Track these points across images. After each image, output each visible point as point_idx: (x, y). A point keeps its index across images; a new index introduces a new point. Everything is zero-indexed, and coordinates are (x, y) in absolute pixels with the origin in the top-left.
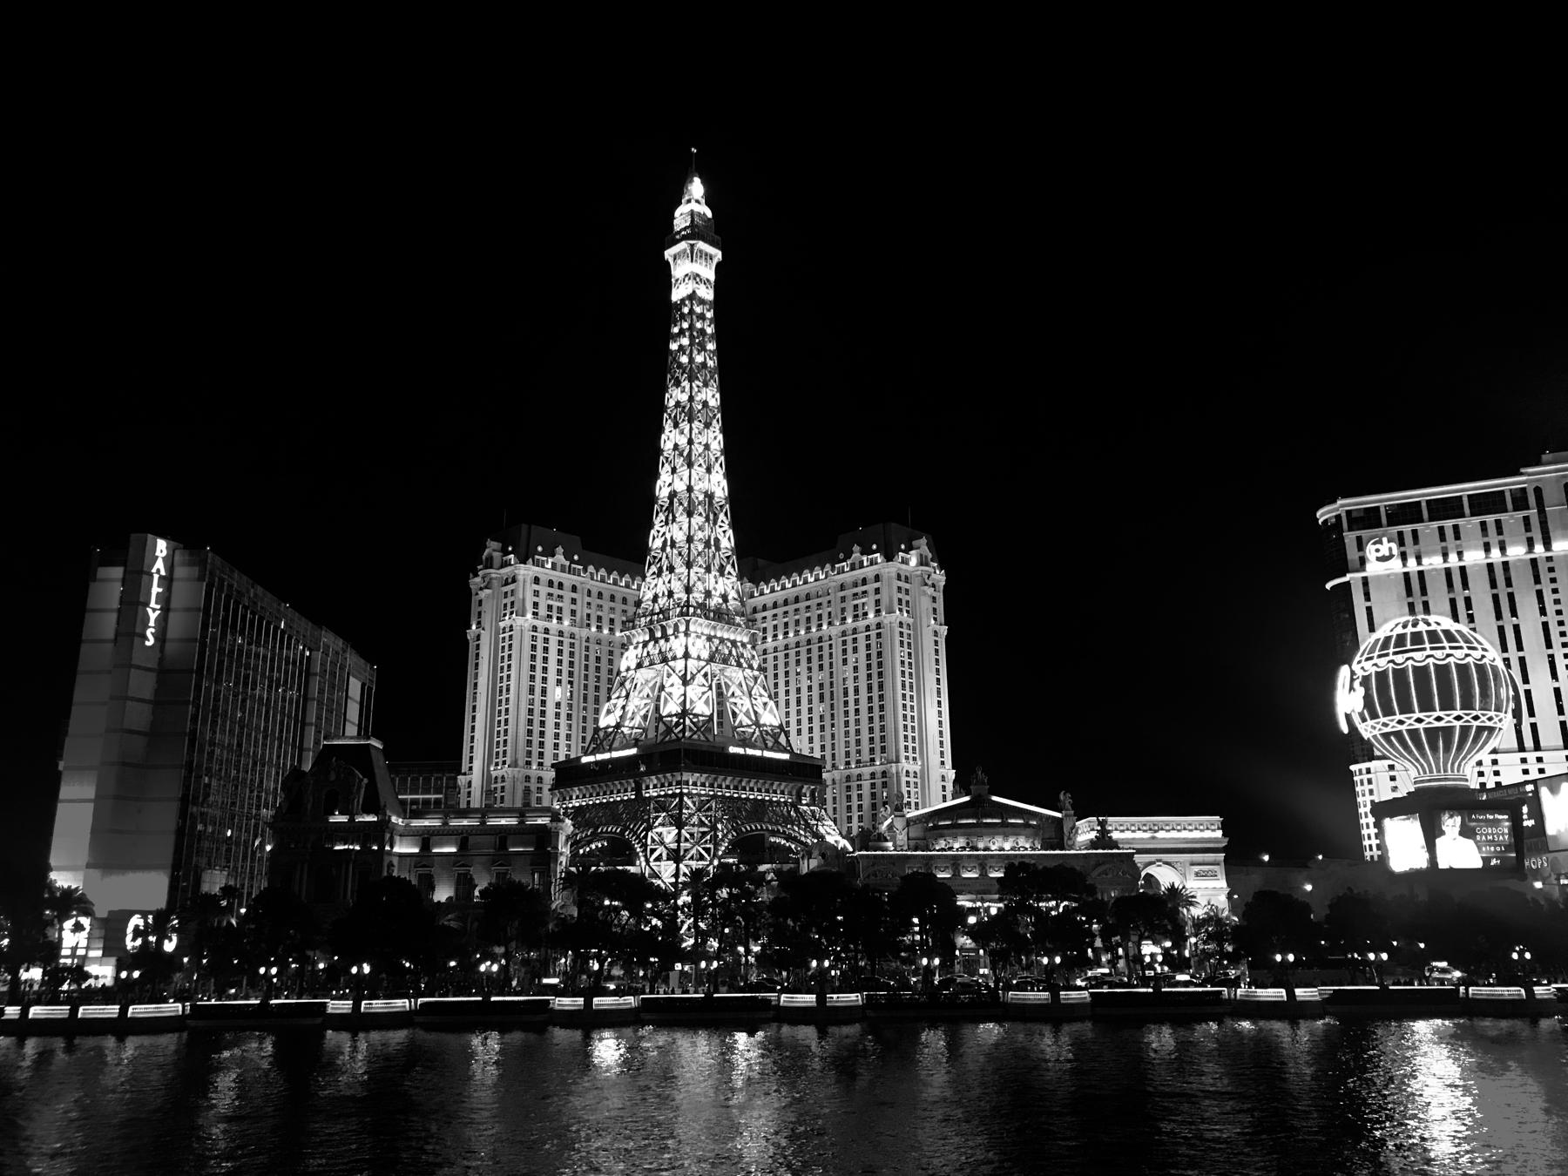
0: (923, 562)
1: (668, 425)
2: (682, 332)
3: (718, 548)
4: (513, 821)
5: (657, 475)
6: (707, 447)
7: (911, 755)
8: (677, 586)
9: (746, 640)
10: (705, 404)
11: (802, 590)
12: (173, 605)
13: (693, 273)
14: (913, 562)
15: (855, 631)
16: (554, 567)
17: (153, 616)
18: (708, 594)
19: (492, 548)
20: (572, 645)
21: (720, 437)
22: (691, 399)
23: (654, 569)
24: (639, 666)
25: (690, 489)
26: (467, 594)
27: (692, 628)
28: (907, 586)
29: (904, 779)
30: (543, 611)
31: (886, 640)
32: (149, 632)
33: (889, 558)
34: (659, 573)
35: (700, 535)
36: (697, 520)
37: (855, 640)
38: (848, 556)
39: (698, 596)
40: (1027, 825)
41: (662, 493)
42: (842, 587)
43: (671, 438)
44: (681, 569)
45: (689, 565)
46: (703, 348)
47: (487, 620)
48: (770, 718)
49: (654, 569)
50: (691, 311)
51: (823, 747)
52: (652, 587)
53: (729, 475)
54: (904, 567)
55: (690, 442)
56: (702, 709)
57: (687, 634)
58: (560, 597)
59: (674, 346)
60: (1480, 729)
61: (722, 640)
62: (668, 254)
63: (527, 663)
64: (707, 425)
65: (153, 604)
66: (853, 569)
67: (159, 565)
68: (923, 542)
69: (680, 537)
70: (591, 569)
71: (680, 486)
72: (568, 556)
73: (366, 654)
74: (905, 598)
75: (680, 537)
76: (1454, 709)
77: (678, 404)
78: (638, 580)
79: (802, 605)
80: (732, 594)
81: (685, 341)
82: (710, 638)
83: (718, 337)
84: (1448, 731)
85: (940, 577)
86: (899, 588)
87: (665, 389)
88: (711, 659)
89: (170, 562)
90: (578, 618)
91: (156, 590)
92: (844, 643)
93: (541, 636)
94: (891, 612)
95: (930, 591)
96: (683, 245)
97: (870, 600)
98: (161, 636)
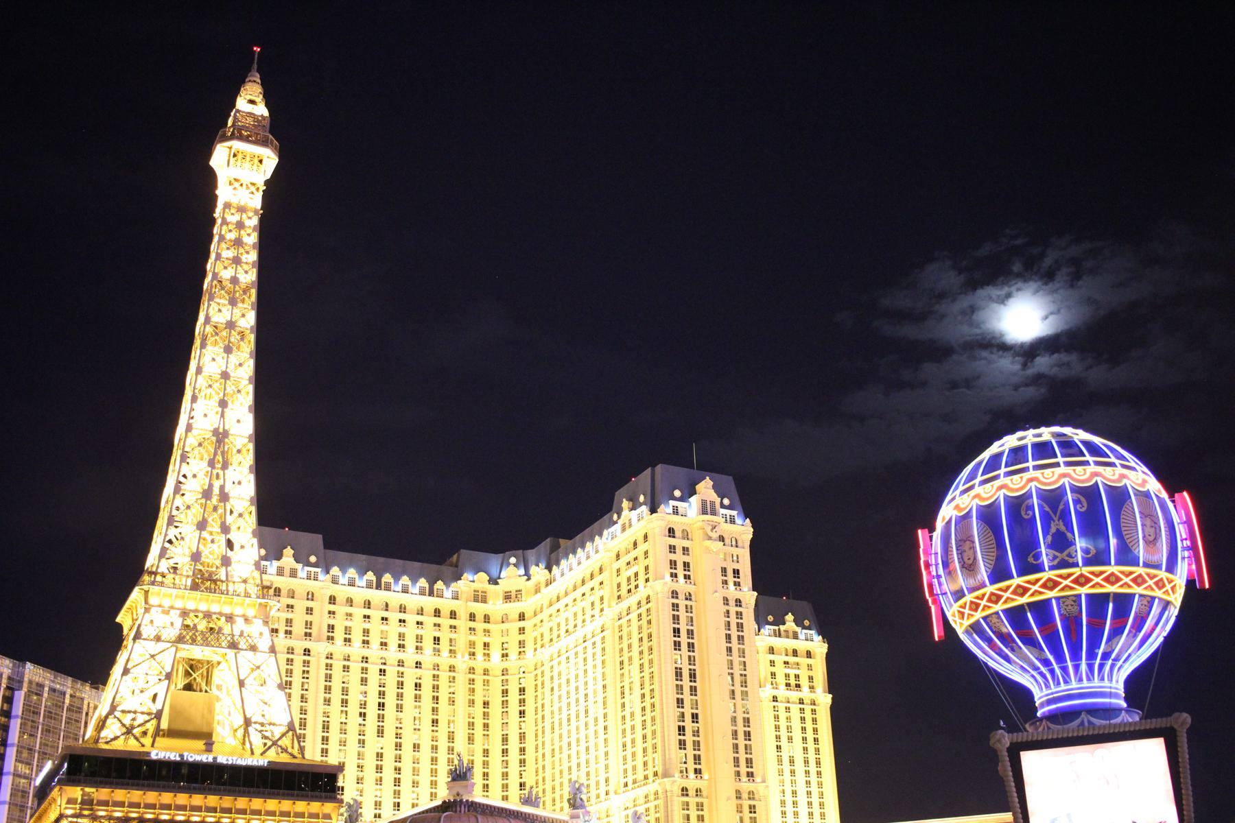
3: (224, 497)
6: (225, 376)
9: (251, 613)
16: (280, 572)
20: (306, 663)
27: (152, 600)
28: (686, 543)
33: (653, 510)
38: (619, 517)
58: (290, 607)
60: (1097, 602)
64: (228, 350)
68: (706, 488)
70: (335, 570)
74: (680, 558)
76: (1039, 568)
83: (264, 246)
84: (1042, 609)
85: (744, 530)
86: (672, 549)
88: (180, 639)
90: (314, 631)
92: (620, 626)
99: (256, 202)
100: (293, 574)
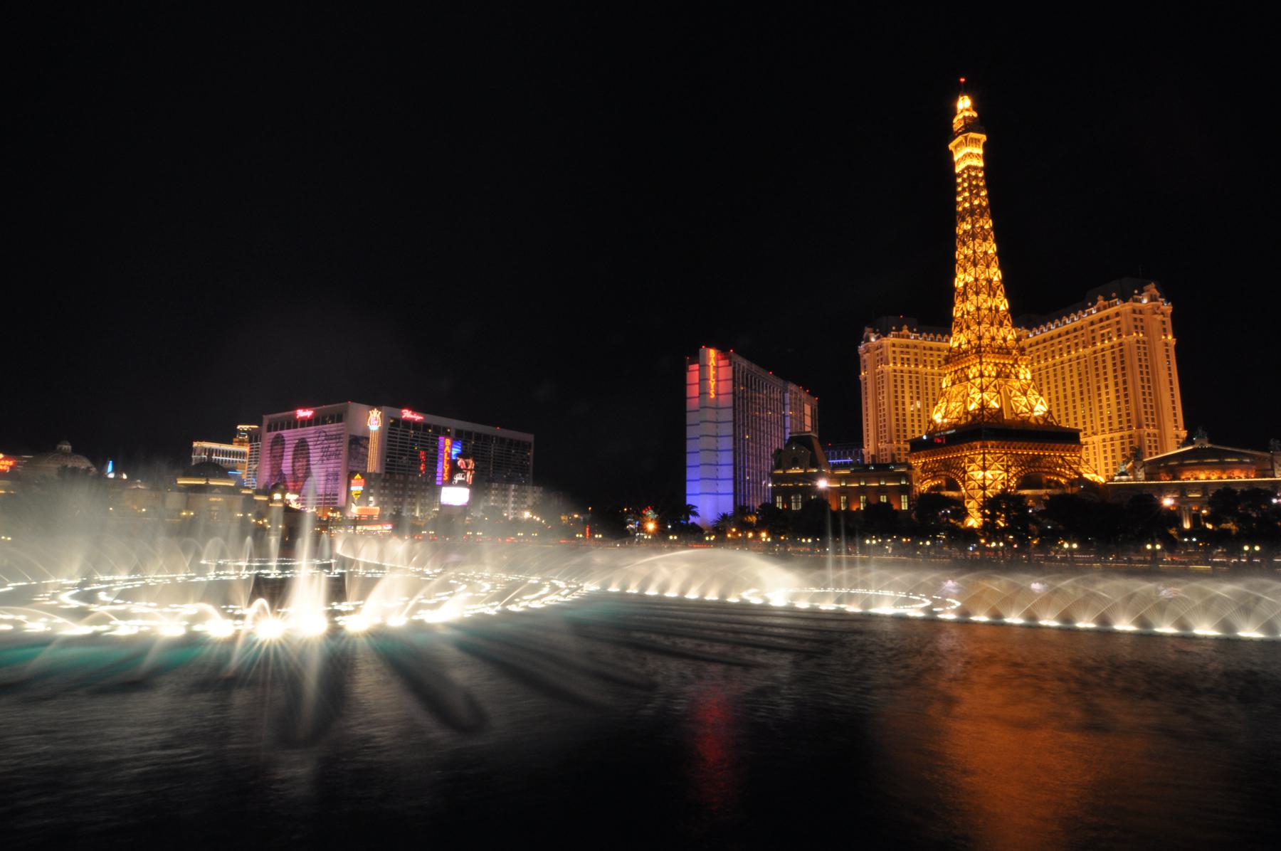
0: (1152, 299)
1: (959, 245)
2: (964, 190)
5: (954, 275)
6: (986, 253)
7: (1150, 423)
8: (973, 337)
10: (982, 228)
11: (1063, 329)
13: (968, 155)
14: (1145, 301)
15: (1103, 350)
17: (712, 384)
18: (993, 339)
19: (868, 330)
21: (994, 246)
22: (973, 227)
23: (958, 329)
24: (954, 383)
25: (976, 280)
26: (857, 357)
29: (1147, 438)
30: (898, 360)
31: (1126, 353)
32: (712, 392)
34: (961, 331)
35: (985, 306)
36: (982, 297)
38: (1094, 303)
39: (985, 341)
40: (1241, 463)
41: (959, 283)
43: (962, 253)
44: (974, 327)
45: (979, 324)
46: (978, 195)
47: (869, 367)
48: (1040, 409)
49: (958, 329)
50: (969, 176)
52: (958, 340)
53: (1001, 267)
55: (975, 252)
56: (994, 404)
57: (981, 363)
59: (959, 199)
61: (1004, 364)
62: (951, 146)
63: (892, 389)
64: (985, 240)
66: (1098, 310)
68: (1152, 288)
69: (972, 309)
71: (970, 279)
72: (911, 330)
73: (812, 394)
74: (1139, 324)
75: (972, 309)
77: (965, 231)
78: (946, 337)
79: (1063, 338)
80: (1009, 337)
81: (967, 194)
82: (996, 364)
83: (987, 186)
85: (1167, 308)
87: (954, 225)
88: (997, 376)
89: (717, 360)
91: (712, 372)
93: (899, 374)
94: (1129, 334)
95: (1160, 317)
96: (960, 138)
97: (1113, 329)
98: (717, 394)
99: (981, 164)
100: (908, 337)
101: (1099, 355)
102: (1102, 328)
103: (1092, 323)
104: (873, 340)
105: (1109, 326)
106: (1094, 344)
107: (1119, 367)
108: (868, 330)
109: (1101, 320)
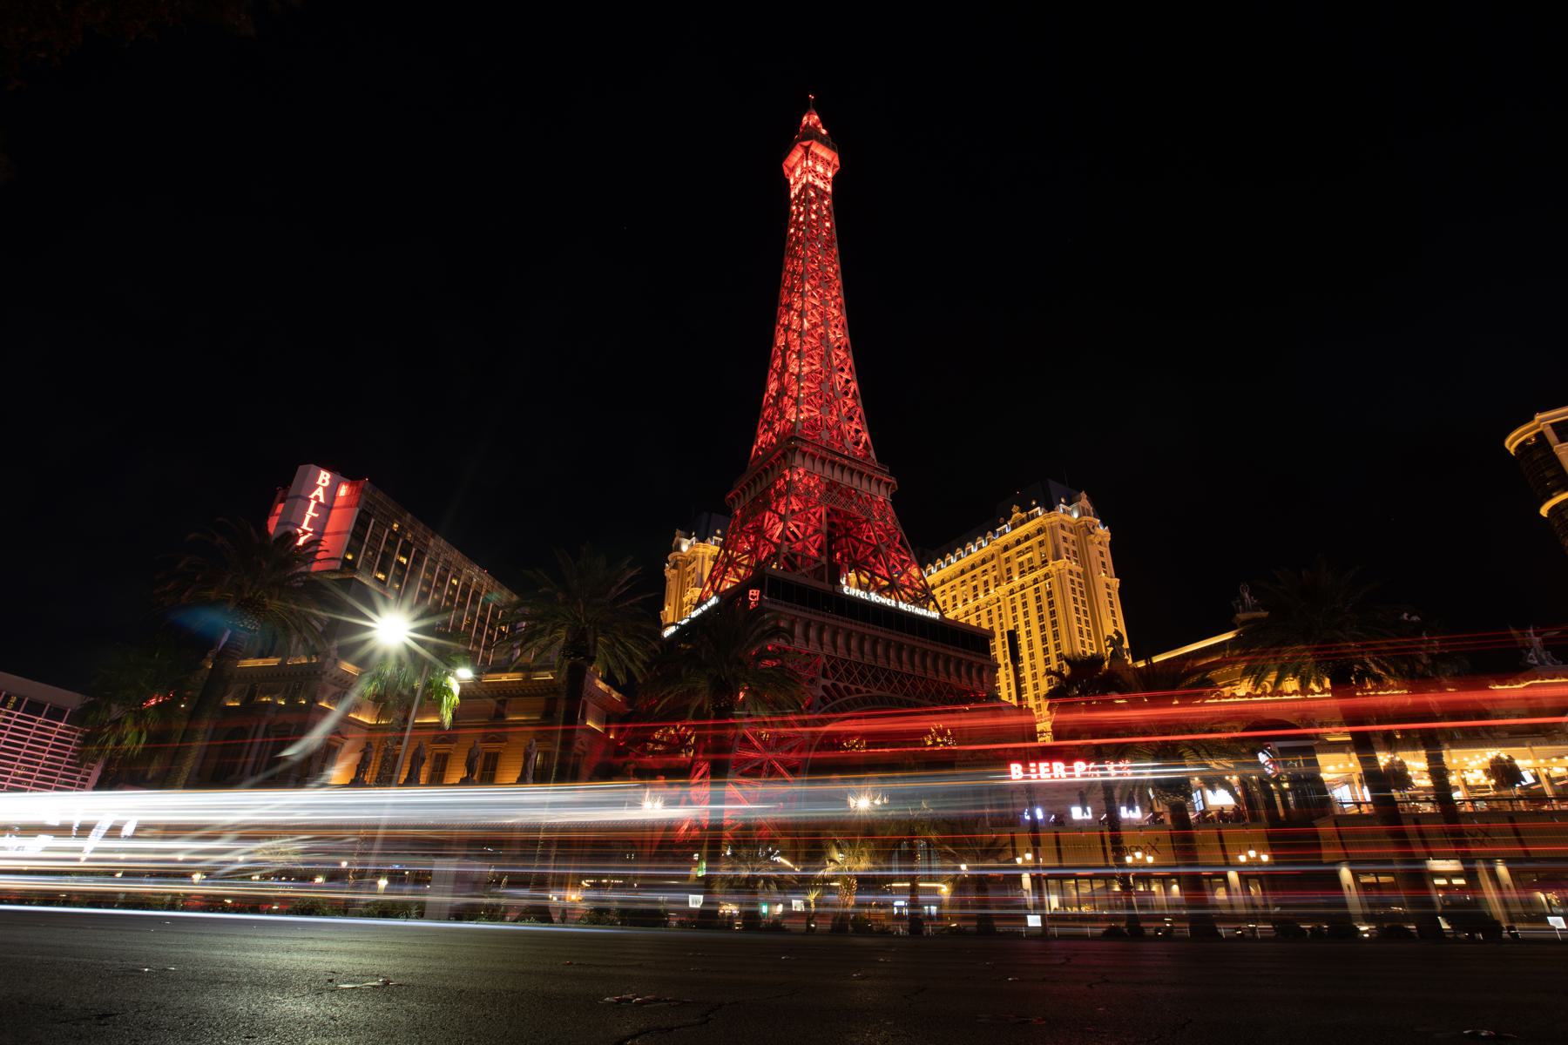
0: (1083, 513)
4: (515, 677)
11: (966, 561)
12: (330, 528)
14: (1076, 515)
15: (1022, 587)
19: (678, 532)
37: (1023, 596)
38: (1008, 516)
42: (1006, 548)
51: (990, 621)
54: (1066, 517)
65: (305, 526)
66: (1014, 527)
67: (320, 492)
89: (331, 492)
92: (1013, 600)
101: (1017, 596)
102: (1020, 554)
103: (1006, 548)
104: (684, 548)
105: (1029, 549)
106: (1010, 579)
107: (1048, 621)
108: (678, 532)
109: (1018, 542)
